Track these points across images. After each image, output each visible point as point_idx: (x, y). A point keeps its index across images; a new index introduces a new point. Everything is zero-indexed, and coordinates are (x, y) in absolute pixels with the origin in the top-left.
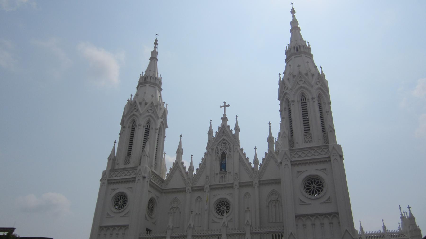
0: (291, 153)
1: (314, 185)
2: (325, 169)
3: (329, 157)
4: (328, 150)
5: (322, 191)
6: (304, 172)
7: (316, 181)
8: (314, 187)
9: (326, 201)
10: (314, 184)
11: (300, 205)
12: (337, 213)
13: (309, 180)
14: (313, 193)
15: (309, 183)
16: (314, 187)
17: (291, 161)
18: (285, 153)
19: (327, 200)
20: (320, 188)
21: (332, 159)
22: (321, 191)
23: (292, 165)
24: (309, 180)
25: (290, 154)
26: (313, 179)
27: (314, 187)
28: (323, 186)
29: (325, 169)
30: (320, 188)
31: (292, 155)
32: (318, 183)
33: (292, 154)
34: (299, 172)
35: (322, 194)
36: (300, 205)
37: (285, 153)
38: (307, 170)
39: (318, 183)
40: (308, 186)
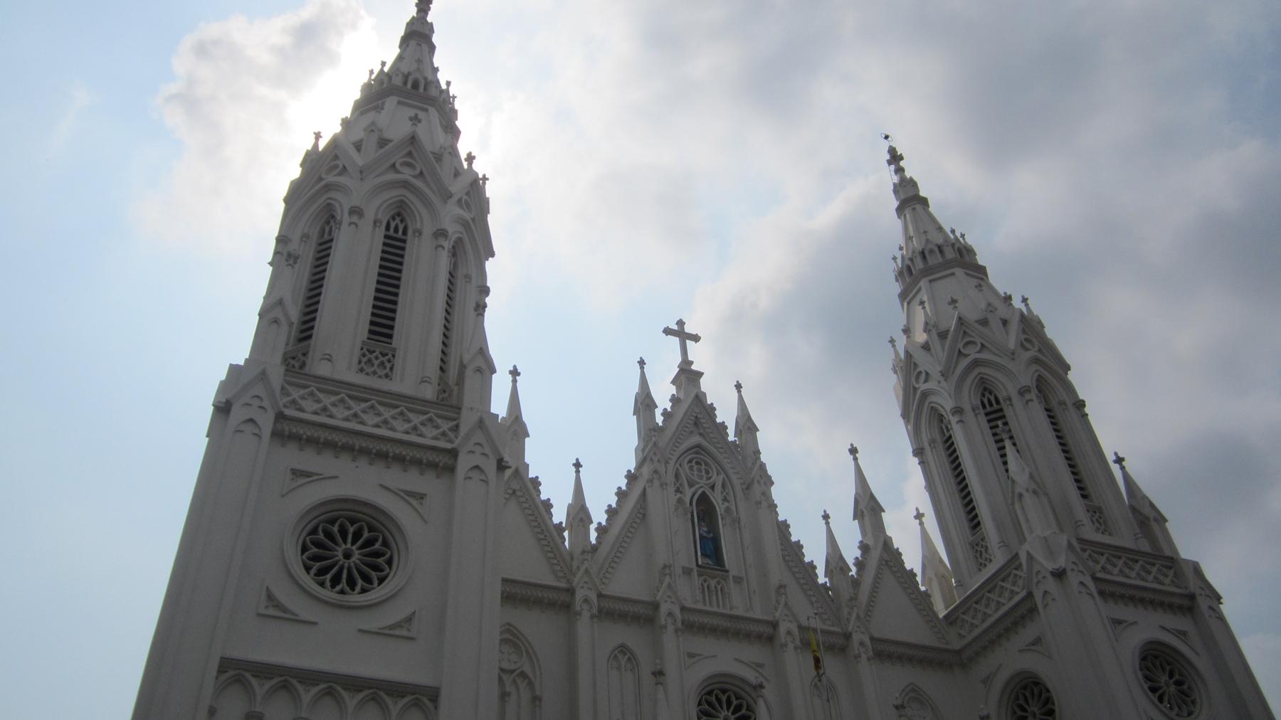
0: (285, 384)
1: (357, 552)
2: (421, 497)
3: (454, 453)
4: (456, 429)
5: (381, 581)
6: (324, 478)
7: (366, 535)
8: (347, 555)
9: (391, 627)
10: (353, 544)
11: (260, 615)
12: (433, 695)
13: (332, 522)
14: (335, 581)
15: (329, 535)
16: (347, 555)
17: (280, 416)
18: (264, 373)
19: (398, 625)
20: (377, 568)
21: (464, 464)
22: (376, 582)
23: (276, 434)
24: (332, 522)
25: (283, 388)
26: (353, 521)
27: (349, 554)
28: (390, 562)
29: (422, 498)
30: (377, 568)
31: (288, 395)
32: (370, 543)
33: (290, 389)
34: (297, 473)
35: (376, 594)
36: (260, 615)
37: (264, 373)
38: (336, 477)
39: (370, 543)
40: (318, 544)
